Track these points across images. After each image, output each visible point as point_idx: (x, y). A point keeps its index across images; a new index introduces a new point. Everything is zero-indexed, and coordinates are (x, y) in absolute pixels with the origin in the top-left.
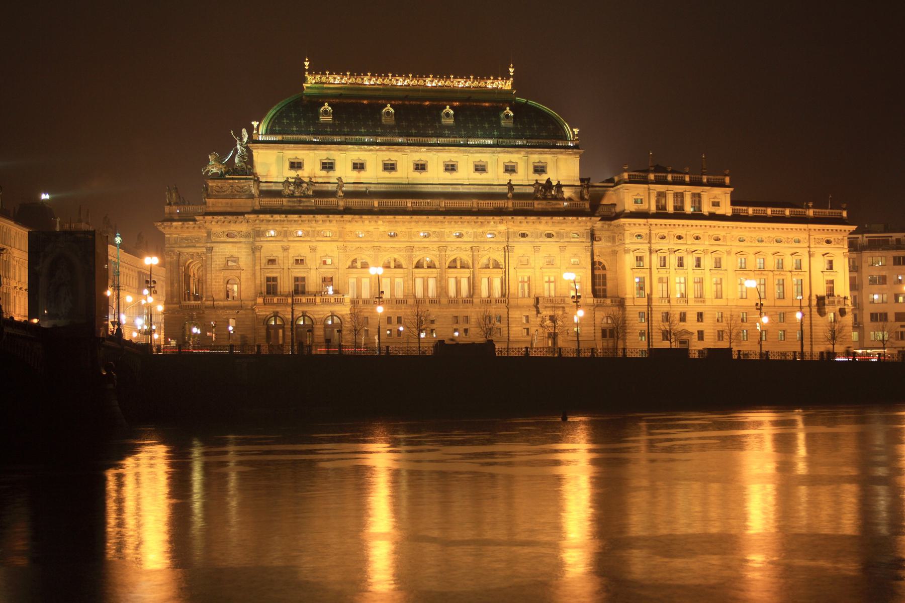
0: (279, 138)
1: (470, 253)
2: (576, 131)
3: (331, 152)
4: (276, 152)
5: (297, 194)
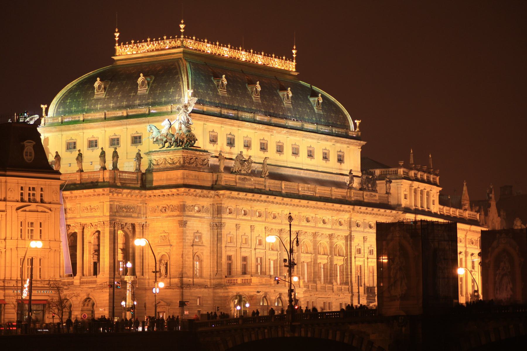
0: (216, 110)
1: (328, 240)
2: (357, 122)
3: (233, 128)
4: (201, 123)
5: (243, 172)
